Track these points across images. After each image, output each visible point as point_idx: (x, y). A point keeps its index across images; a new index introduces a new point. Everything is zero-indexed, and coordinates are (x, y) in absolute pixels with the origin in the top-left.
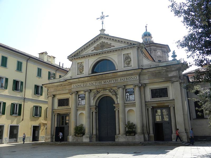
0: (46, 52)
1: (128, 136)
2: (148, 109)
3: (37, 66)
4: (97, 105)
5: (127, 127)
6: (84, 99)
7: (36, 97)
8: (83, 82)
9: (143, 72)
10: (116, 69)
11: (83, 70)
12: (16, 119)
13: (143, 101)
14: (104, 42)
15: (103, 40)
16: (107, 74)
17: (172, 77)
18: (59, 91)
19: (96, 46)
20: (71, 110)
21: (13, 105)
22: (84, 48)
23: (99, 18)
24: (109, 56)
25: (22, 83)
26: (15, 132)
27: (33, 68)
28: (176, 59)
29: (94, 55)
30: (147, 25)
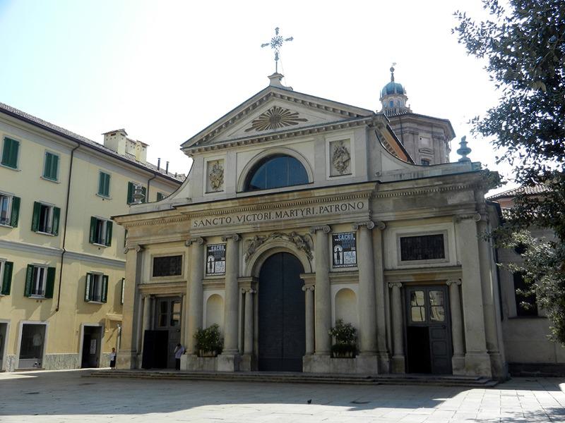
0: (123, 131)
1: (336, 360)
2: (391, 290)
3: (99, 167)
4: (257, 275)
5: (334, 334)
6: (223, 259)
7: (93, 251)
8: (222, 212)
9: (381, 190)
10: (310, 180)
11: (221, 182)
12: (40, 307)
13: (380, 268)
14: (281, 108)
16: (285, 195)
17: (456, 206)
18: (156, 234)
19: (258, 119)
20: (186, 287)
21: (32, 270)
22: (227, 124)
23: (267, 44)
24: (291, 147)
25: (57, 211)
26: (36, 343)
27: (86, 173)
28: (468, 160)
29: (252, 141)
30: (394, 64)
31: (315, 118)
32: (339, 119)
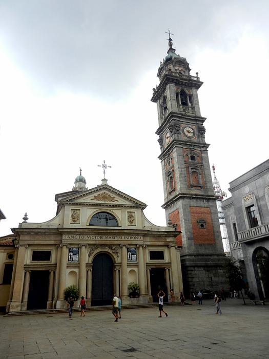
1: (132, 299)
15: (106, 192)
31: (121, 202)
32: (131, 204)
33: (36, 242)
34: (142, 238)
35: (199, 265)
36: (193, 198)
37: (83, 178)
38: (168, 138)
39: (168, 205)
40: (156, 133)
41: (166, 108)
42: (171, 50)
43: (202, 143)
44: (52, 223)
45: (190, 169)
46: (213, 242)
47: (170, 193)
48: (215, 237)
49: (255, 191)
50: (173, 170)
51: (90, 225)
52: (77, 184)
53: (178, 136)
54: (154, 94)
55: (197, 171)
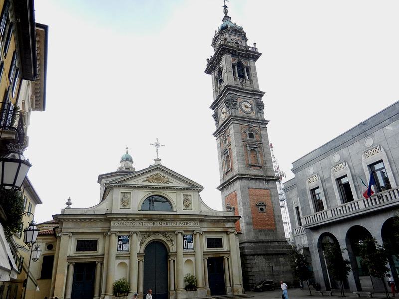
6: (127, 243)
15: (159, 173)
31: (176, 184)
32: (186, 186)
33: (81, 230)
34: (199, 223)
35: (259, 253)
36: (252, 179)
37: (130, 157)
38: (224, 113)
39: (225, 187)
40: (211, 107)
41: (221, 81)
42: (227, 18)
43: (260, 119)
44: (98, 208)
45: (248, 148)
46: (273, 227)
47: (227, 174)
48: (274, 223)
49: (320, 173)
50: (230, 149)
51: (141, 210)
52: (123, 163)
53: (235, 112)
54: (208, 66)
55: (256, 149)
